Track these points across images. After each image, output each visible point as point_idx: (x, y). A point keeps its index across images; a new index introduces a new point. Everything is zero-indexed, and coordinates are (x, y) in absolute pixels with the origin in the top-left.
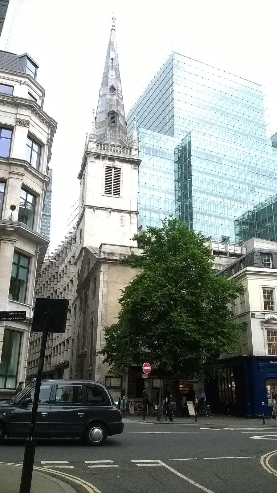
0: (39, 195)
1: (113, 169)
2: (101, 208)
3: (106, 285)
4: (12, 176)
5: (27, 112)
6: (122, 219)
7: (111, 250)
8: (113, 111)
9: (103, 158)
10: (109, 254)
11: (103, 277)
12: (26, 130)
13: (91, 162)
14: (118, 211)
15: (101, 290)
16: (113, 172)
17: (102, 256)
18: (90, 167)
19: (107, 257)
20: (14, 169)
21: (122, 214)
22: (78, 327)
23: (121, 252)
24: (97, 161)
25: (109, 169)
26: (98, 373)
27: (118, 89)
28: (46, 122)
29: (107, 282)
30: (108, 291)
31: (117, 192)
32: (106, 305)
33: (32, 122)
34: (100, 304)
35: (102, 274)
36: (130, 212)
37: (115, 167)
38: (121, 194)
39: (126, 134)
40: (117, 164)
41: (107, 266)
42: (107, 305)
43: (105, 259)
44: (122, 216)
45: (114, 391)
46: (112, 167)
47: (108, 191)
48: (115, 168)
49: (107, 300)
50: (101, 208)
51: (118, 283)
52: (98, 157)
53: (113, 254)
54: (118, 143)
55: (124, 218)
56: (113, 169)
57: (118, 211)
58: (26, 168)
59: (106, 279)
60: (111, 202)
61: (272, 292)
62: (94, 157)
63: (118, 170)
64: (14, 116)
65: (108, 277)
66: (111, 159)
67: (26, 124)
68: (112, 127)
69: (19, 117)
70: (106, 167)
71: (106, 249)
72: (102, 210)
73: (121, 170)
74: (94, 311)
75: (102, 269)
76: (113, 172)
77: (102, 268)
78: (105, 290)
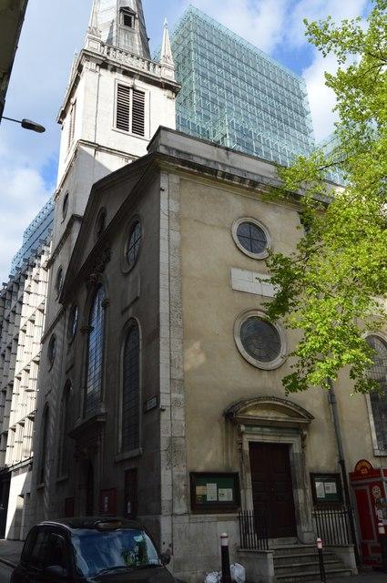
1: (131, 91)
3: (177, 224)
8: (128, 8)
9: (114, 69)
13: (91, 70)
15: (163, 234)
18: (88, 77)
22: (64, 372)
24: (103, 71)
25: (122, 89)
26: (170, 461)
30: (183, 239)
34: (163, 269)
35: (164, 195)
37: (137, 88)
40: (140, 85)
41: (175, 179)
45: (219, 519)
46: (128, 88)
47: (121, 124)
52: (104, 65)
59: (174, 208)
62: (97, 64)
65: (180, 207)
66: (127, 73)
70: (119, 85)
72: (111, 153)
73: (146, 96)
75: (163, 184)
78: (175, 236)
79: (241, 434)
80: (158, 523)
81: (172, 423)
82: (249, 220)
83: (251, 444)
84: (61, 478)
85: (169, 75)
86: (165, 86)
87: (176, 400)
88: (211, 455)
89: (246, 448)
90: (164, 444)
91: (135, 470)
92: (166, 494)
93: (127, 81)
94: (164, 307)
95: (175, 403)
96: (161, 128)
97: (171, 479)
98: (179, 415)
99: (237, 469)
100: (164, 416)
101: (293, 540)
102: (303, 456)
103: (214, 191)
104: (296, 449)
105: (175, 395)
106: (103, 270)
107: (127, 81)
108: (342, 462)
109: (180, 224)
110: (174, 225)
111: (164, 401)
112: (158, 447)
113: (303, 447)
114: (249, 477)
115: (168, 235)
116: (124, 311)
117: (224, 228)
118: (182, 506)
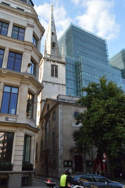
0: (37, 63)
1: (54, 66)
2: (50, 82)
4: (26, 51)
5: (33, 21)
6: (59, 88)
7: (63, 98)
8: (54, 42)
9: (50, 61)
10: (62, 99)
11: (60, 111)
12: (32, 29)
14: (57, 84)
15: (59, 117)
16: (54, 67)
17: (59, 100)
19: (61, 101)
20: (27, 47)
22: (41, 137)
23: (68, 99)
24: (48, 62)
25: (52, 66)
27: (55, 34)
28: (40, 29)
29: (62, 113)
31: (56, 76)
32: (62, 125)
33: (34, 27)
36: (62, 85)
38: (58, 77)
39: (59, 52)
40: (57, 64)
41: (62, 105)
42: (63, 124)
43: (61, 102)
44: (59, 86)
47: (52, 75)
48: (55, 65)
49: (63, 121)
50: (50, 82)
51: (67, 114)
53: (64, 100)
54: (56, 55)
55: (60, 87)
56: (54, 66)
57: (57, 84)
58: (33, 47)
60: (54, 80)
64: (27, 22)
66: (54, 61)
67: (32, 27)
68: (53, 49)
69: (28, 22)
71: (61, 97)
73: (58, 67)
74: (55, 128)
75: (60, 107)
76: (54, 67)
77: (60, 106)
78: (62, 117)
79: (73, 154)
80: (58, 169)
81: (61, 152)
82: (76, 112)
83: (75, 156)
84: (41, 160)
85: (64, 60)
86: (63, 63)
87: (62, 148)
88: (68, 157)
89: (74, 156)
90: (59, 156)
91: (55, 160)
92: (60, 164)
93: (53, 63)
94: (59, 131)
95: (61, 149)
96: (59, 95)
97: (60, 162)
98: (62, 151)
99: (72, 160)
100: (60, 151)
101: (82, 172)
102: (85, 157)
103: (69, 106)
104: (83, 156)
105: (61, 147)
106: (49, 118)
107: (53, 63)
108: (93, 159)
109: (62, 115)
110: (62, 115)
111: (60, 148)
112: (58, 156)
113: (85, 156)
114: (74, 161)
115: (60, 117)
116: (53, 129)
117: (71, 114)
118: (62, 166)
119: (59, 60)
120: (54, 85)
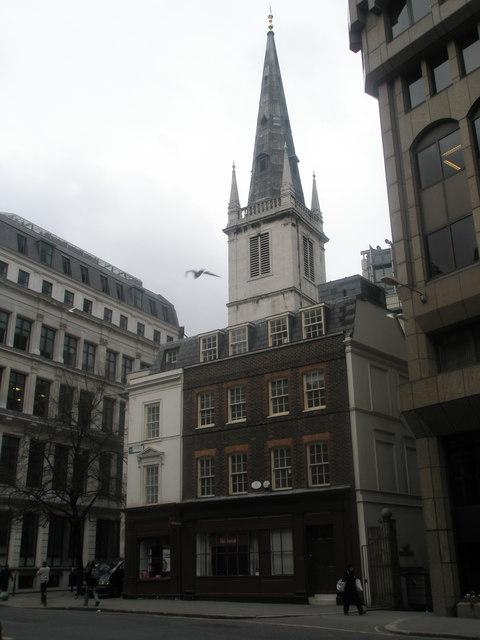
2: (245, 301)
6: (273, 306)
9: (246, 229)
14: (267, 296)
21: (275, 298)
24: (239, 236)
25: (253, 240)
31: (266, 269)
36: (282, 292)
40: (264, 228)
47: (254, 273)
50: (245, 301)
57: (267, 296)
61: (158, 408)
63: (265, 236)
66: (256, 225)
93: (253, 232)
107: (253, 232)
119: (272, 212)
120: (257, 302)
